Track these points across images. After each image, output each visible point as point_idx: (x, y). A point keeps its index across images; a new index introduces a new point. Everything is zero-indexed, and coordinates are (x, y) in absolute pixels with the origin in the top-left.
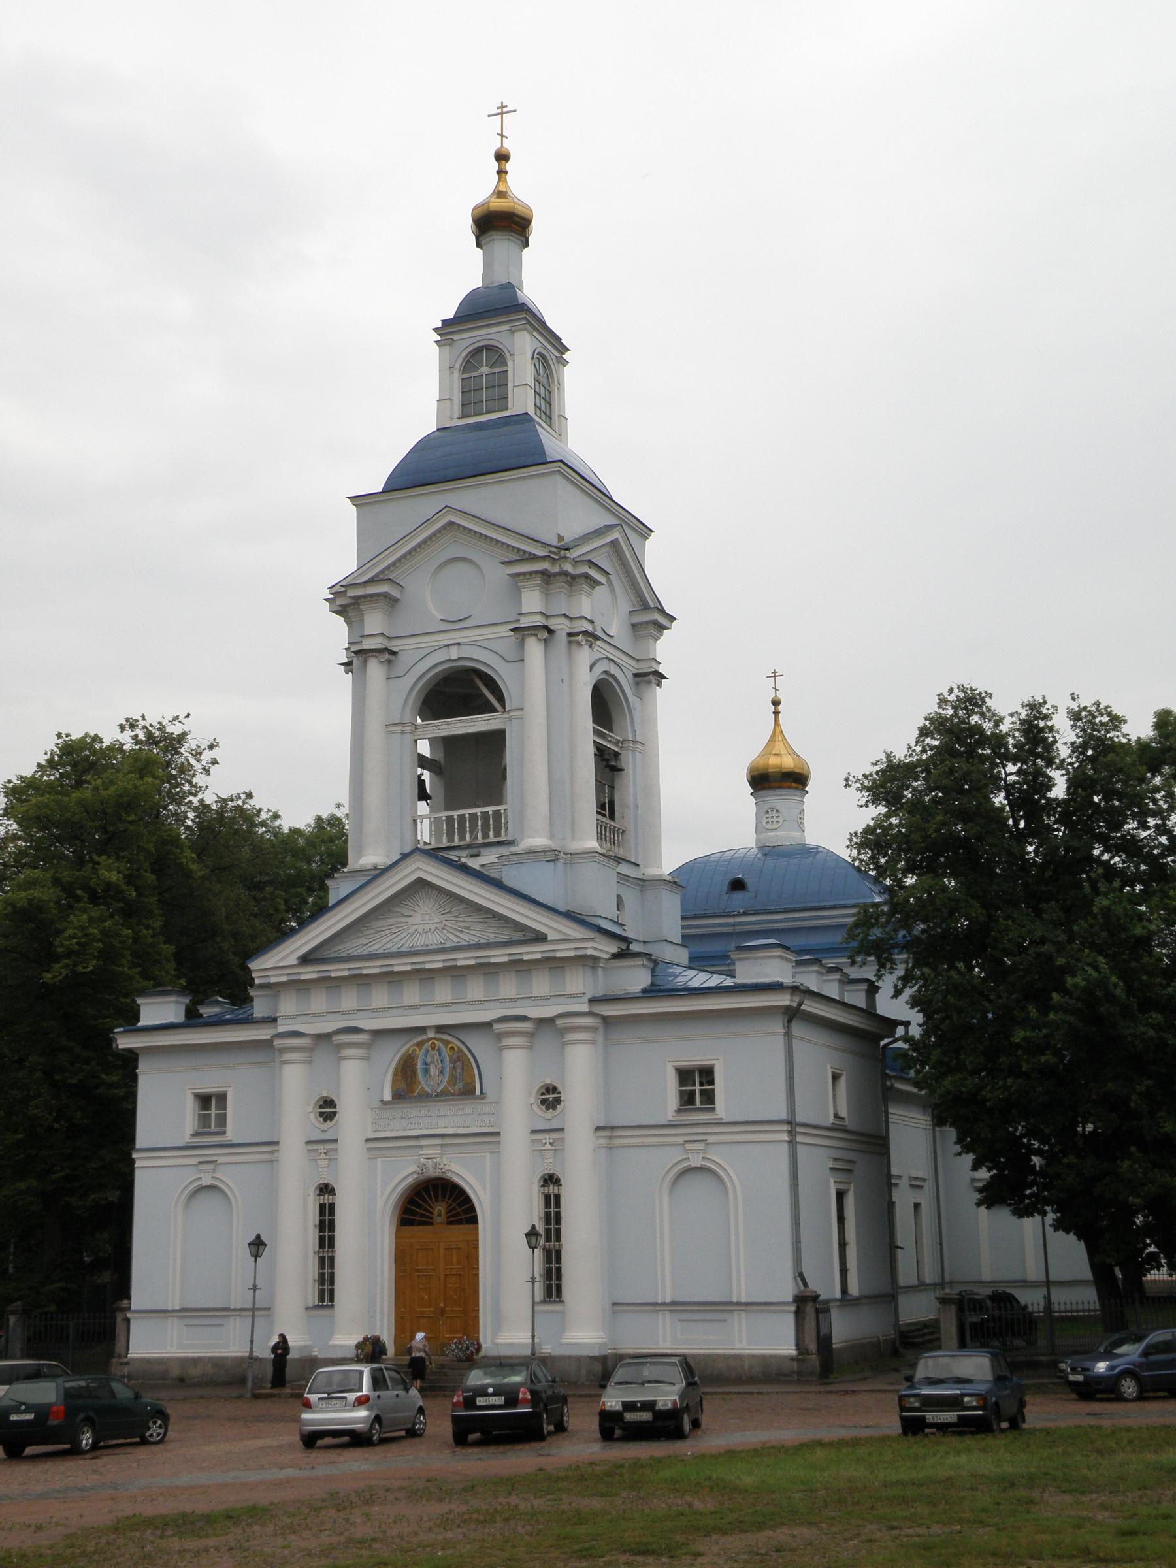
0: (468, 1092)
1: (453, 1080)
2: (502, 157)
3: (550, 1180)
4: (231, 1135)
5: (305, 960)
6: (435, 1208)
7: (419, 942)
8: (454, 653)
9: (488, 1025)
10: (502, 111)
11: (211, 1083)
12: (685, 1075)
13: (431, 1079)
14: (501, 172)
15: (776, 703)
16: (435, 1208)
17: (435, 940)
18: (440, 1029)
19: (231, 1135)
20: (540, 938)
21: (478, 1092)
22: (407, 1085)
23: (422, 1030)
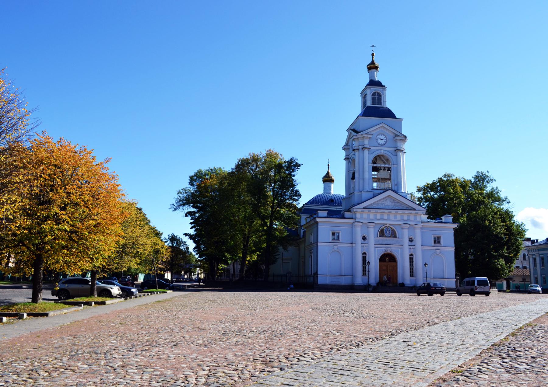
0: (395, 237)
1: (392, 235)
2: (373, 55)
3: (411, 255)
4: (341, 241)
5: (364, 208)
6: (388, 259)
7: (387, 207)
8: (382, 152)
9: (400, 225)
10: (373, 46)
11: (336, 229)
12: (435, 238)
13: (387, 234)
14: (373, 58)
15: (328, 165)
16: (388, 259)
17: (390, 207)
18: (389, 224)
19: (341, 241)
20: (415, 210)
21: (397, 236)
22: (382, 233)
23: (386, 224)
